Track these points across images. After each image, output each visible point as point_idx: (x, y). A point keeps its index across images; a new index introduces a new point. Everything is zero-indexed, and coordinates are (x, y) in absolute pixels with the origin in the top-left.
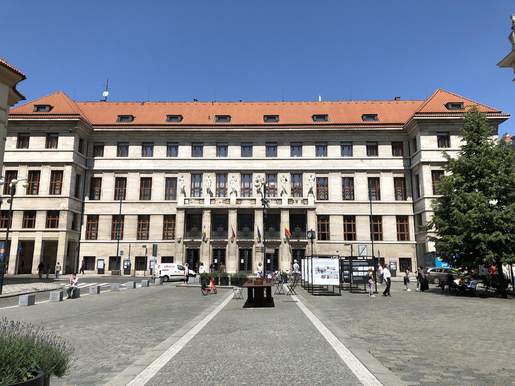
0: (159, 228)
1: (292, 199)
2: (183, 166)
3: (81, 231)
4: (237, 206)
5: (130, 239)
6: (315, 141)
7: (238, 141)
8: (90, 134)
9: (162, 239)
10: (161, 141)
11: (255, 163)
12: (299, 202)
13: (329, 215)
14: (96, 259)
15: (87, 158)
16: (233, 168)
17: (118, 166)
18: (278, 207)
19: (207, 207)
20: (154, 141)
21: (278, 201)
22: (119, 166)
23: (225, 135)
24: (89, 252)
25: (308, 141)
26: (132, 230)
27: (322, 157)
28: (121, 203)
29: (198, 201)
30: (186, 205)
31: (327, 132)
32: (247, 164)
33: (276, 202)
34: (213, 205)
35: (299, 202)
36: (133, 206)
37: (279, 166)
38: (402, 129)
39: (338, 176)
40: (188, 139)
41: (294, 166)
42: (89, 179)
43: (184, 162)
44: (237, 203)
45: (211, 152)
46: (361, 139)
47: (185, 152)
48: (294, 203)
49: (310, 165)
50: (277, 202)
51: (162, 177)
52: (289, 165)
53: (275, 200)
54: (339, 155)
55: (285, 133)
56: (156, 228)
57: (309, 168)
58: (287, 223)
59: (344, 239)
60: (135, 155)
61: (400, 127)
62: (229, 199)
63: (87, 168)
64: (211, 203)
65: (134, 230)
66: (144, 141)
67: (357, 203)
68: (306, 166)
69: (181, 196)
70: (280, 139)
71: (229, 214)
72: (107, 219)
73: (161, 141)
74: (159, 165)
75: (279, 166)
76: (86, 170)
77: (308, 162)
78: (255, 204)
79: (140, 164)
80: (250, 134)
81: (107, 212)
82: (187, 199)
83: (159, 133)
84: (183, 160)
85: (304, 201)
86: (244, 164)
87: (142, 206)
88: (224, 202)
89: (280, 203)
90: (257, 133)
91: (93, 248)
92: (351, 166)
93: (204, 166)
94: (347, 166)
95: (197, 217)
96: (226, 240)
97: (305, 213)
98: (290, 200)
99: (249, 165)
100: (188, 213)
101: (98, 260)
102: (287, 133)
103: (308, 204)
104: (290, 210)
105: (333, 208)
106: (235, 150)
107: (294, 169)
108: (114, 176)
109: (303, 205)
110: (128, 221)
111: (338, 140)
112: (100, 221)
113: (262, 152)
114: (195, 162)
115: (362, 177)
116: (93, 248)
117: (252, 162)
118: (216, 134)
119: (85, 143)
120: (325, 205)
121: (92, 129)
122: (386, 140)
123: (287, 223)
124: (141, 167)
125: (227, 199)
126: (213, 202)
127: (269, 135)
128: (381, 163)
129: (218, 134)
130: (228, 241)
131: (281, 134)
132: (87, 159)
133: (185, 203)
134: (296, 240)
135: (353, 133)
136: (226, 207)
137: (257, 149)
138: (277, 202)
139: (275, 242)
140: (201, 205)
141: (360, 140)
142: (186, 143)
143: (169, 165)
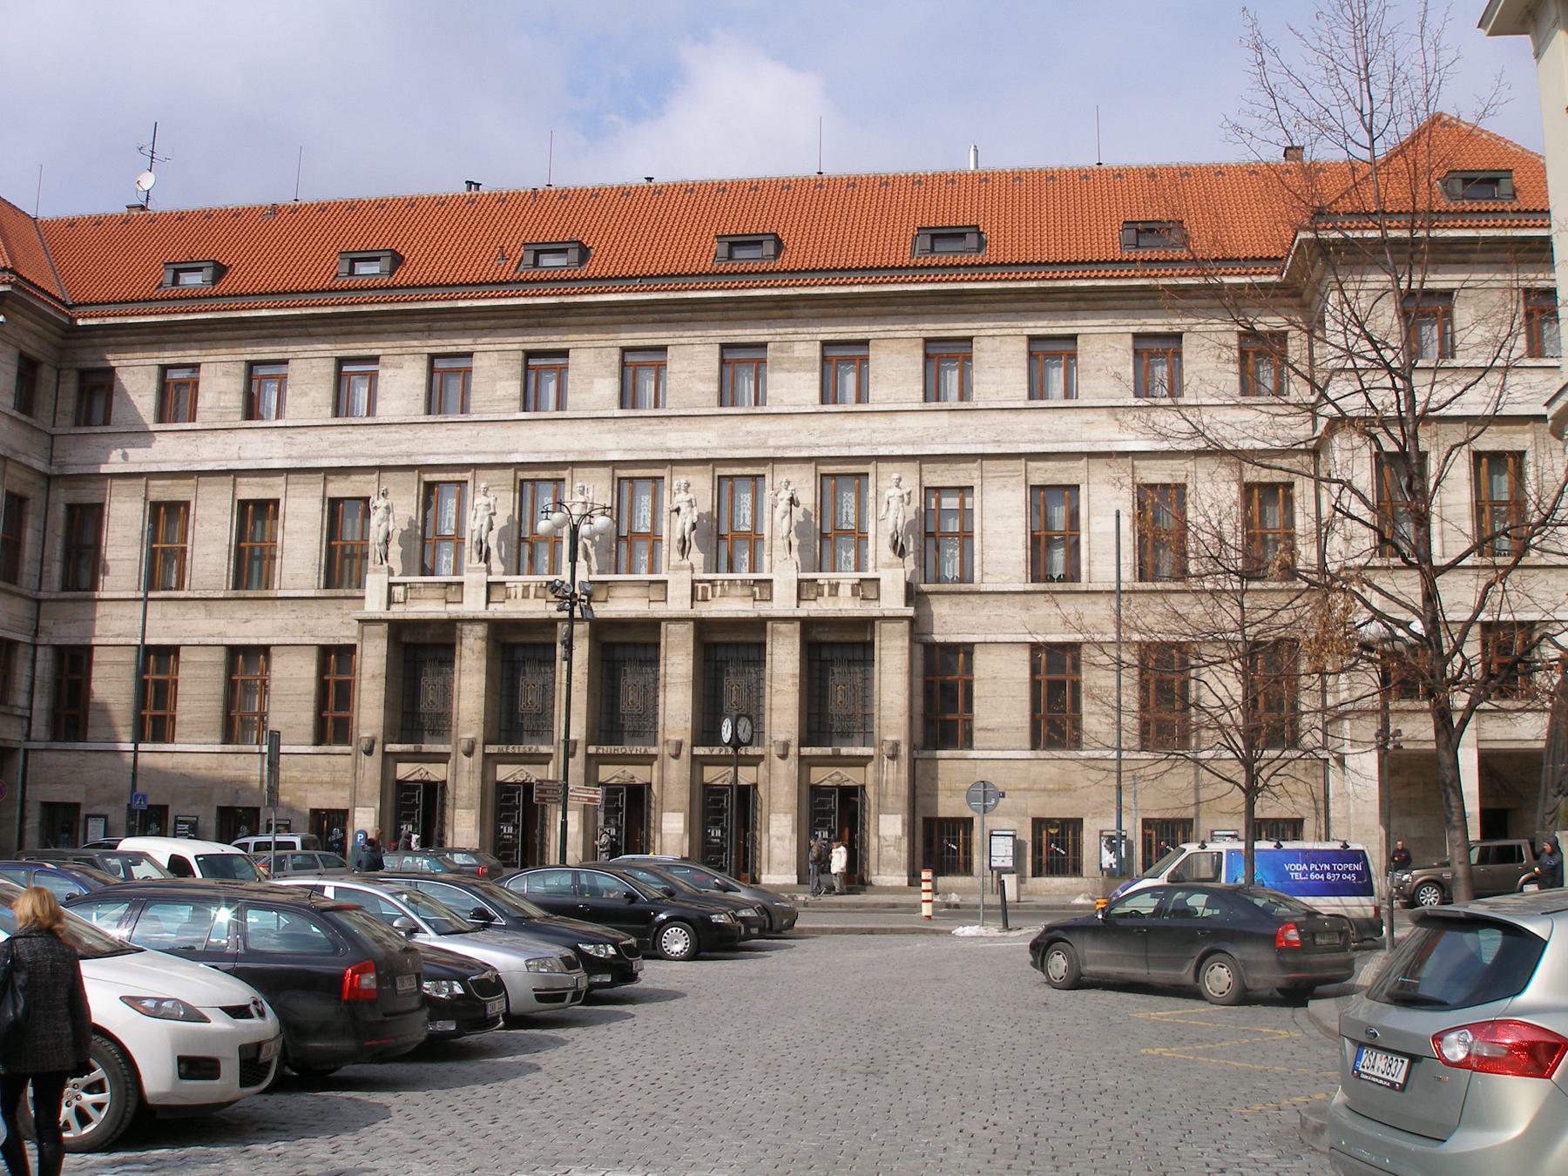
0: (303, 698)
2: (395, 449)
3: (31, 708)
5: (199, 740)
8: (64, 338)
9: (310, 740)
11: (678, 431)
12: (845, 590)
13: (972, 644)
14: (83, 812)
15: (54, 431)
16: (585, 453)
17: (159, 457)
19: (470, 616)
20: (286, 356)
21: (756, 589)
22: (164, 457)
24: (59, 787)
26: (203, 704)
28: (146, 600)
29: (441, 592)
30: (394, 608)
31: (972, 298)
32: (642, 437)
33: (747, 591)
34: (500, 607)
35: (845, 590)
36: (209, 614)
37: (771, 442)
38: (1274, 278)
39: (1013, 481)
41: (834, 442)
42: (59, 512)
43: (397, 435)
45: (500, 393)
47: (404, 395)
49: (898, 436)
50: (753, 595)
52: (812, 440)
54: (1018, 393)
55: (797, 307)
56: (290, 698)
58: (790, 681)
59: (1028, 745)
60: (221, 415)
61: (1269, 274)
63: (55, 471)
64: (488, 602)
65: (209, 704)
66: (254, 357)
67: (1087, 592)
68: (882, 441)
69: (376, 571)
72: (117, 663)
74: (306, 448)
76: (49, 478)
77: (894, 425)
78: (666, 600)
79: (236, 447)
80: (654, 313)
81: (119, 636)
82: (398, 584)
84: (393, 428)
86: (631, 436)
87: (242, 611)
88: (540, 593)
89: (766, 596)
90: (684, 307)
91: (73, 772)
92: (1071, 437)
93: (473, 448)
94: (1052, 437)
98: (805, 589)
101: (88, 816)
102: (805, 307)
103: (878, 599)
104: (807, 624)
105: (989, 617)
106: (596, 380)
107: (832, 454)
108: (146, 499)
110: (193, 672)
112: (97, 672)
113: (702, 387)
114: (440, 435)
116: (73, 772)
117: (661, 427)
118: (523, 317)
119: (47, 374)
120: (957, 604)
121: (66, 320)
123: (790, 681)
124: (239, 458)
126: (497, 594)
127: (732, 314)
130: (552, 751)
131: (781, 308)
132: (53, 436)
133: (390, 601)
134: (828, 751)
135: (1079, 299)
137: (683, 376)
138: (753, 595)
140: (451, 607)
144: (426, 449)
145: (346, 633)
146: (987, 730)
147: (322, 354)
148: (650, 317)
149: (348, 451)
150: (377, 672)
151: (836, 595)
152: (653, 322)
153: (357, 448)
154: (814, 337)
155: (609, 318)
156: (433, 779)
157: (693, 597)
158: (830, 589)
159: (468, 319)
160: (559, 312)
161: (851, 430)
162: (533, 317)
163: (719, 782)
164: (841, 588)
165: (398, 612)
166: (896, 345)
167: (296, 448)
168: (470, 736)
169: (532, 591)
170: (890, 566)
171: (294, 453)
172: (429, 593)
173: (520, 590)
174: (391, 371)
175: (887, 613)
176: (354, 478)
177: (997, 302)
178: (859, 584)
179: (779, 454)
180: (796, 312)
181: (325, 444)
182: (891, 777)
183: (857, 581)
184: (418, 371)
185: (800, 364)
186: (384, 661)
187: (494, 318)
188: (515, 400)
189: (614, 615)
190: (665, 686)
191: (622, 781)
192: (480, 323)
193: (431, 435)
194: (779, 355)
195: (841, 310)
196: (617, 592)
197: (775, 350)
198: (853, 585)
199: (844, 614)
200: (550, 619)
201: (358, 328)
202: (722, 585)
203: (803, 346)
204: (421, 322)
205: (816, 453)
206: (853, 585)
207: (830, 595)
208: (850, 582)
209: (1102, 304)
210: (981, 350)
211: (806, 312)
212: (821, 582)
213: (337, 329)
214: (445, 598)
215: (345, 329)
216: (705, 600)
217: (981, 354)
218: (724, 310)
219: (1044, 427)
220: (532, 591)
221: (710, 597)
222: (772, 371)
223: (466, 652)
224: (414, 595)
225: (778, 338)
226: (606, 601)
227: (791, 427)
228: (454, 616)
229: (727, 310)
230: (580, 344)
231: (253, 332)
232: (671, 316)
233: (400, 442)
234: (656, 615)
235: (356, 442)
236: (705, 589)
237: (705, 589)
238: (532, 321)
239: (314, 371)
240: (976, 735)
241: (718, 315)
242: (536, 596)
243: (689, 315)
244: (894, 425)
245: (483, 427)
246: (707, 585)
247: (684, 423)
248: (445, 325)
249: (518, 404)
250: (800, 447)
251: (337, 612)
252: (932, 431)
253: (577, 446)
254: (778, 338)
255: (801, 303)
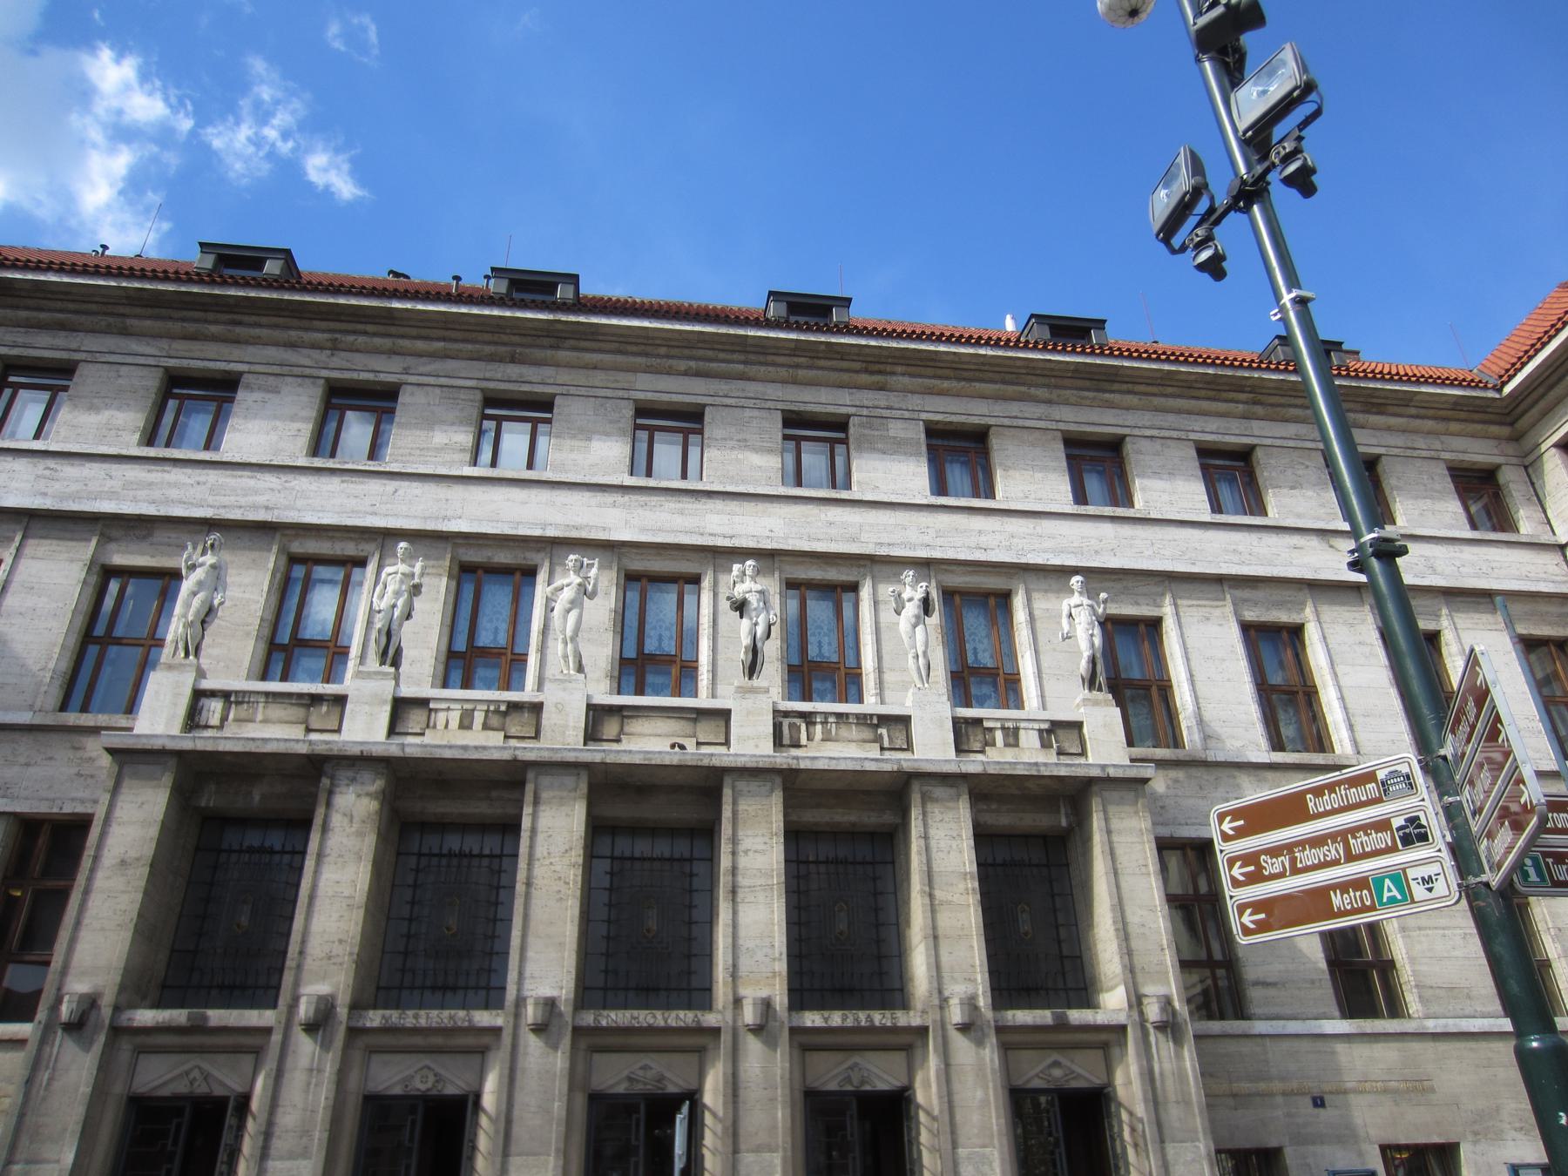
1: (978, 722)
2: (243, 501)
4: (596, 754)
6: (1062, 426)
7: (620, 393)
10: (130, 359)
12: (1029, 739)
18: (895, 769)
19: (356, 751)
21: (883, 731)
23: (539, 354)
25: (1020, 423)
27: (1108, 511)
29: (299, 712)
33: (867, 734)
35: (1029, 739)
40: (307, 362)
43: (252, 482)
44: (591, 735)
46: (1298, 438)
48: (994, 744)
49: (1048, 544)
50: (879, 739)
51: (72, 561)
52: (927, 539)
53: (863, 720)
55: (893, 373)
57: (1046, 556)
58: (961, 886)
62: (537, 708)
64: (392, 731)
70: (866, 403)
71: (527, 810)
73: (130, 359)
74: (74, 487)
75: (864, 537)
77: (1039, 530)
78: (727, 743)
82: (213, 694)
83: (123, 315)
85: (1060, 732)
88: (495, 721)
95: (275, 839)
96: (483, 1018)
97: (1064, 823)
98: (965, 733)
99: (679, 521)
100: (209, 799)
103: (1083, 753)
109: (1052, 757)
111: (1182, 435)
114: (330, 487)
115: (1352, 625)
122: (1416, 453)
125: (514, 707)
126: (415, 719)
127: (801, 373)
128: (1427, 559)
129: (496, 343)
130: (499, 1022)
131: (872, 373)
133: (193, 720)
134: (1044, 1016)
135: (1255, 403)
136: (506, 756)
138: (879, 739)
139: (884, 1030)
141: (1291, 443)
142: (290, 379)
143: (142, 494)
144: (299, 503)
145: (80, 795)
146: (1266, 984)
147: (142, 360)
148: (682, 365)
149: (157, 494)
150: (133, 854)
151: (1017, 745)
152: (686, 373)
153: (174, 493)
154: (915, 415)
155: (620, 358)
156: (218, 1091)
157: (778, 742)
158: (1006, 736)
159: (403, 337)
160: (546, 341)
161: (980, 531)
162: (505, 344)
163: (833, 1086)
164: (1022, 732)
165: (203, 741)
166: (1025, 434)
167: (57, 486)
168: (324, 989)
169: (479, 717)
170: (1096, 703)
171: (50, 491)
172: (277, 711)
173: (455, 717)
174: (257, 396)
175: (1112, 773)
176: (160, 535)
177: (1154, 395)
178: (1049, 731)
179: (883, 551)
180: (892, 380)
181: (115, 484)
182: (1167, 1066)
183: (1045, 726)
184: (305, 399)
185: (897, 448)
186: (154, 832)
187: (444, 339)
188: (463, 450)
189: (637, 760)
190: (734, 892)
191: (638, 1088)
192: (420, 345)
193: (314, 487)
194: (866, 432)
195: (954, 384)
196: (636, 726)
197: (861, 425)
198: (1040, 731)
199: (1045, 772)
200: (515, 761)
201: (214, 329)
202: (824, 723)
203: (900, 424)
204: (323, 331)
205: (937, 554)
206: (1040, 731)
207: (1006, 745)
208: (1036, 726)
209: (1282, 411)
210: (1139, 452)
211: (906, 380)
212: (987, 724)
213: (176, 327)
214: (305, 722)
215: (191, 328)
216: (797, 745)
217: (1142, 457)
218: (790, 366)
219: (1241, 548)
220: (479, 717)
221: (804, 740)
222: (860, 449)
223: (337, 820)
224: (243, 715)
225: (865, 412)
226: (618, 741)
227: (892, 521)
228: (321, 749)
229: (797, 366)
230: (573, 390)
231: (23, 314)
232: (714, 365)
233: (256, 492)
234: (716, 762)
235: (176, 485)
236: (791, 726)
237: (795, 729)
238: (502, 349)
239: (120, 381)
240: (1254, 994)
241: (783, 372)
242: (486, 727)
243: (741, 367)
244: (1039, 530)
245: (405, 487)
246: (797, 721)
247: (733, 505)
248: (361, 339)
249: (467, 457)
250: (904, 545)
251: (71, 754)
252: (1093, 541)
253: (558, 518)
254: (865, 412)
255: (899, 369)
